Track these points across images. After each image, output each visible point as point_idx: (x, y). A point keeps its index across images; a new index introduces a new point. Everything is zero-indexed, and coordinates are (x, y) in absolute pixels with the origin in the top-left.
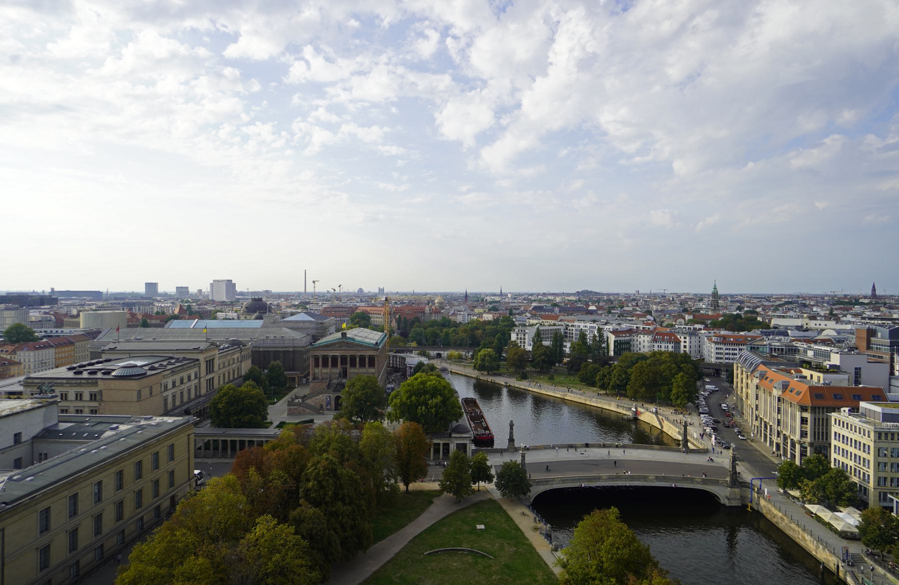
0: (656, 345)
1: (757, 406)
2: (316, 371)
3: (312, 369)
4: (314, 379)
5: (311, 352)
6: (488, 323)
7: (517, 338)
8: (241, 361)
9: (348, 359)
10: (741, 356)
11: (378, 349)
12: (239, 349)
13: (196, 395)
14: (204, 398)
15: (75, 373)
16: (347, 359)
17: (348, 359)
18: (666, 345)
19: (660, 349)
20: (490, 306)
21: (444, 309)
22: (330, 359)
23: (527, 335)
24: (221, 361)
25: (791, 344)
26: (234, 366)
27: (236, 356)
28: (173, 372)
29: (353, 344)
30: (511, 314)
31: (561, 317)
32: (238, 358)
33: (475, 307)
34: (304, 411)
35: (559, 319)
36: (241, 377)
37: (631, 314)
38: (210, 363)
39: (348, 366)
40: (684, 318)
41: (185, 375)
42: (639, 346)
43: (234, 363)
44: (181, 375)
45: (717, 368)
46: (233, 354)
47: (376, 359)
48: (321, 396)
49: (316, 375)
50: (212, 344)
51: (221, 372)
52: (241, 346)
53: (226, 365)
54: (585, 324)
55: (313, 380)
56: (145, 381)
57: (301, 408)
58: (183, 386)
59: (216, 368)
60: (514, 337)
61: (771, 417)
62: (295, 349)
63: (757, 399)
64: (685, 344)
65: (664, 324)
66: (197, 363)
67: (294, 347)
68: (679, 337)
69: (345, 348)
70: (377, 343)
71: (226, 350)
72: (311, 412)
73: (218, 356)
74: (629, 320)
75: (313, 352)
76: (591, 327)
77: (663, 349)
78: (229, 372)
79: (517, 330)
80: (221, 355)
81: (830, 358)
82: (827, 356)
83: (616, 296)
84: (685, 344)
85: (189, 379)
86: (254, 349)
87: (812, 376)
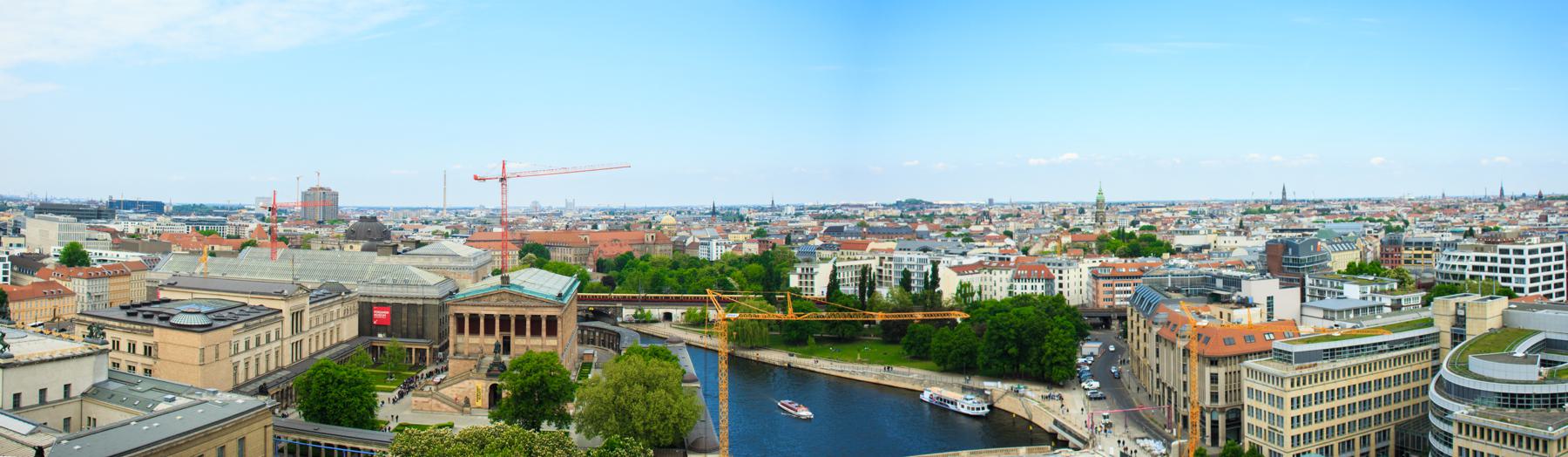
1: (1158, 366)
6: (752, 259)
7: (801, 282)
10: (1136, 294)
13: (277, 367)
14: (289, 372)
15: (129, 314)
18: (1034, 284)
19: (1024, 291)
20: (755, 228)
21: (676, 235)
23: (815, 277)
25: (1196, 272)
26: (332, 324)
27: (335, 309)
28: (246, 326)
30: (788, 241)
33: (729, 231)
35: (868, 250)
37: (983, 236)
38: (297, 316)
41: (262, 332)
42: (994, 288)
43: (332, 321)
44: (257, 332)
45: (1105, 315)
46: (331, 305)
50: (301, 287)
52: (343, 294)
56: (209, 335)
58: (259, 350)
59: (306, 327)
60: (794, 281)
63: (1158, 356)
64: (1061, 281)
65: (1031, 252)
66: (279, 315)
68: (1051, 271)
73: (308, 307)
74: (979, 247)
76: (920, 260)
77: (1029, 291)
78: (324, 334)
79: (799, 270)
80: (313, 305)
81: (1241, 287)
83: (959, 209)
84: (1061, 281)
85: (268, 341)
86: (362, 299)
87: (1221, 313)
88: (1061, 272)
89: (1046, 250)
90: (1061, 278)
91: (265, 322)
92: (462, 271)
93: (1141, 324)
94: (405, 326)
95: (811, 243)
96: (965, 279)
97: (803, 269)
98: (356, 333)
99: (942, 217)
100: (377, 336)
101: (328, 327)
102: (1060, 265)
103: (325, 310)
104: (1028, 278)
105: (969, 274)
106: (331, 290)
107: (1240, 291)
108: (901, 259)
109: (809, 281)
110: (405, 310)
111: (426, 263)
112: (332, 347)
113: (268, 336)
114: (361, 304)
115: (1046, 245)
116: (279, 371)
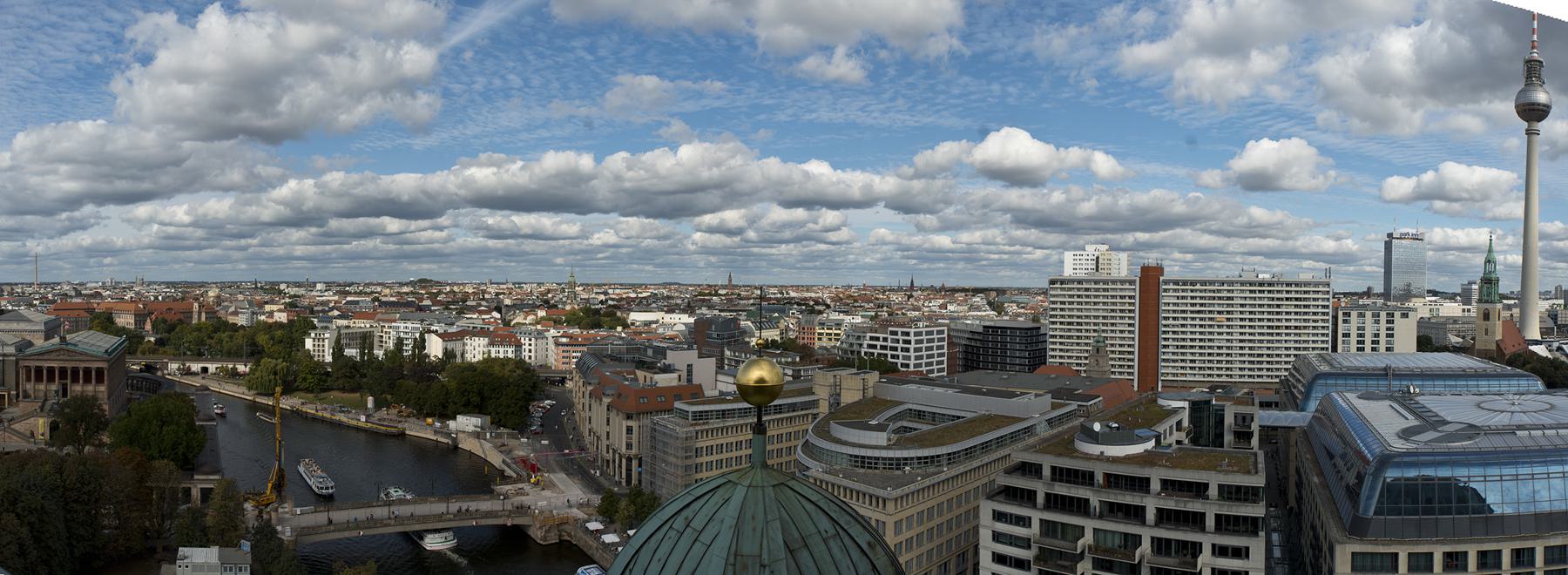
0: (493, 350)
7: (314, 345)
19: (497, 355)
23: (326, 341)
31: (379, 316)
40: (536, 315)
42: (473, 352)
54: (405, 325)
60: (309, 344)
61: (601, 429)
77: (502, 356)
79: (313, 335)
82: (662, 352)
88: (530, 340)
89: (524, 322)
90: (530, 345)
93: (581, 383)
95: (330, 314)
96: (450, 346)
97: (316, 334)
99: (446, 294)
102: (530, 334)
104: (501, 344)
105: (452, 340)
107: (665, 359)
108: (399, 327)
109: (321, 344)
115: (525, 319)
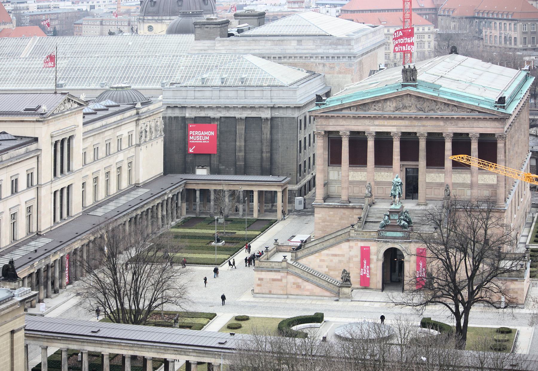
2: (334, 174)
3: (323, 171)
4: (327, 198)
5: (320, 121)
8: (139, 145)
9: (423, 145)
11: (503, 118)
12: (134, 112)
13: (29, 232)
16: (417, 143)
17: (423, 145)
22: (371, 144)
24: (90, 142)
26: (121, 157)
27: (124, 131)
29: (434, 101)
32: (130, 137)
34: (299, 287)
36: (137, 186)
39: (422, 163)
43: (119, 150)
46: (118, 125)
47: (500, 145)
48: (345, 246)
49: (334, 189)
51: (89, 171)
53: (102, 153)
55: (325, 200)
57: (291, 279)
59: (77, 162)
62: (277, 114)
67: (273, 108)
69: (413, 112)
70: (502, 100)
71: (100, 114)
72: (318, 290)
75: (324, 122)
78: (108, 174)
80: (90, 127)
85: (14, 190)
86: (170, 113)
91: (11, 159)
92: (336, 61)
94: (242, 154)
98: (160, 169)
100: (194, 172)
101: (112, 161)
103: (108, 134)
106: (119, 101)
110: (241, 128)
111: (277, 50)
112: (121, 194)
113: (15, 183)
114: (169, 121)
116: (33, 239)
